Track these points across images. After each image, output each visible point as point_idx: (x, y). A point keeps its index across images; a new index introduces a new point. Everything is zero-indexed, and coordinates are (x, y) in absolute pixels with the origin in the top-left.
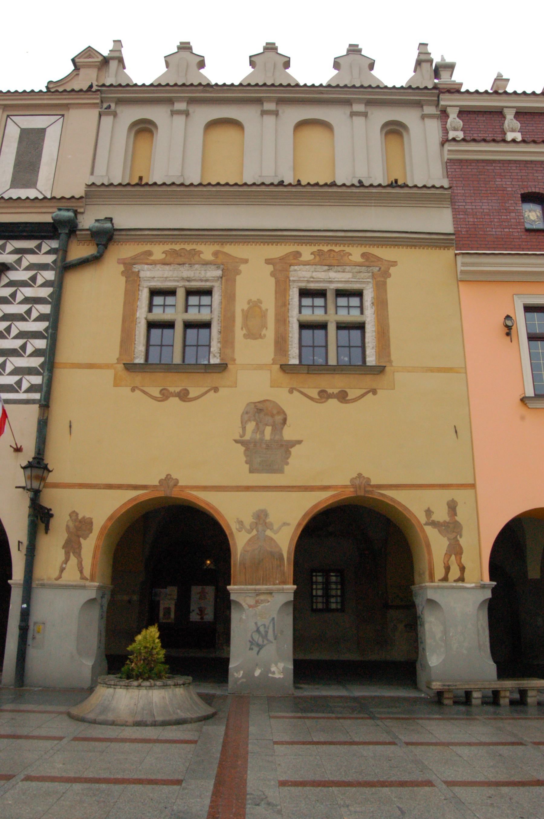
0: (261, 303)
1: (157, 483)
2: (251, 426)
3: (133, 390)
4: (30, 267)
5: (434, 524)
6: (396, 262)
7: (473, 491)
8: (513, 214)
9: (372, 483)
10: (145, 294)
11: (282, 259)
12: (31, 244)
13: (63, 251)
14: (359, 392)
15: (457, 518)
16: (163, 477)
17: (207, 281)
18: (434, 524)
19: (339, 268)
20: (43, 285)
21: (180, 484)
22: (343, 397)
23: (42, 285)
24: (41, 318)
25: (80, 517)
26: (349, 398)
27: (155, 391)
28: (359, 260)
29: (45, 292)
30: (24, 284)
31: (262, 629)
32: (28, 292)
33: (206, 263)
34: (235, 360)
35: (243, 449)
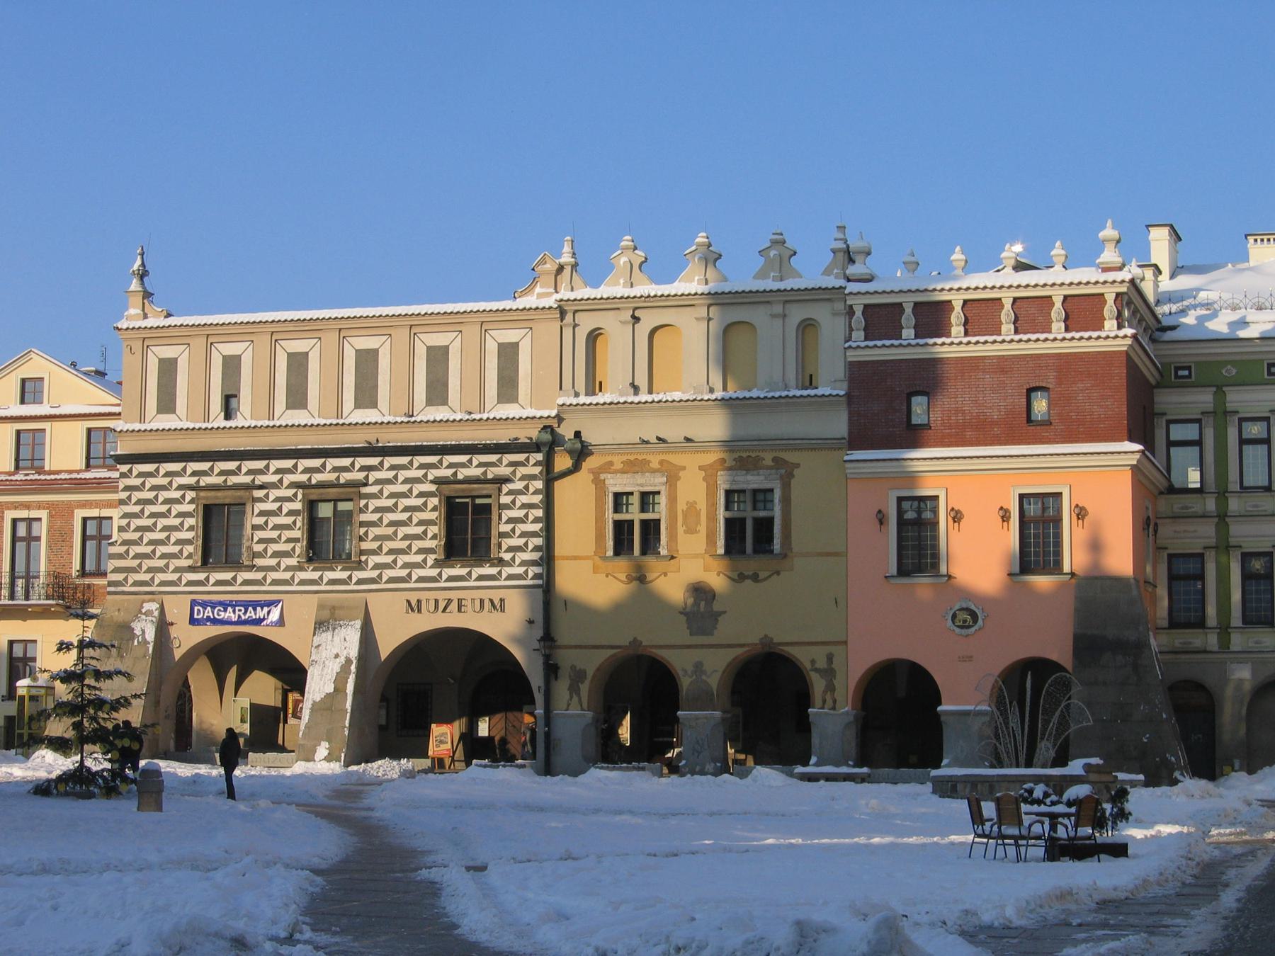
0: (696, 503)
1: (628, 644)
3: (607, 576)
4: (523, 478)
5: (816, 670)
6: (799, 464)
7: (845, 646)
8: (898, 414)
9: (775, 641)
10: (610, 498)
11: (711, 466)
13: (548, 464)
14: (766, 574)
15: (833, 666)
16: (631, 639)
17: (655, 486)
18: (816, 670)
19: (755, 472)
20: (534, 493)
21: (644, 644)
22: (755, 578)
23: (534, 493)
24: (536, 520)
25: (578, 668)
26: (760, 578)
28: (771, 463)
30: (519, 492)
31: (700, 742)
33: (654, 471)
34: (678, 551)
35: (685, 618)
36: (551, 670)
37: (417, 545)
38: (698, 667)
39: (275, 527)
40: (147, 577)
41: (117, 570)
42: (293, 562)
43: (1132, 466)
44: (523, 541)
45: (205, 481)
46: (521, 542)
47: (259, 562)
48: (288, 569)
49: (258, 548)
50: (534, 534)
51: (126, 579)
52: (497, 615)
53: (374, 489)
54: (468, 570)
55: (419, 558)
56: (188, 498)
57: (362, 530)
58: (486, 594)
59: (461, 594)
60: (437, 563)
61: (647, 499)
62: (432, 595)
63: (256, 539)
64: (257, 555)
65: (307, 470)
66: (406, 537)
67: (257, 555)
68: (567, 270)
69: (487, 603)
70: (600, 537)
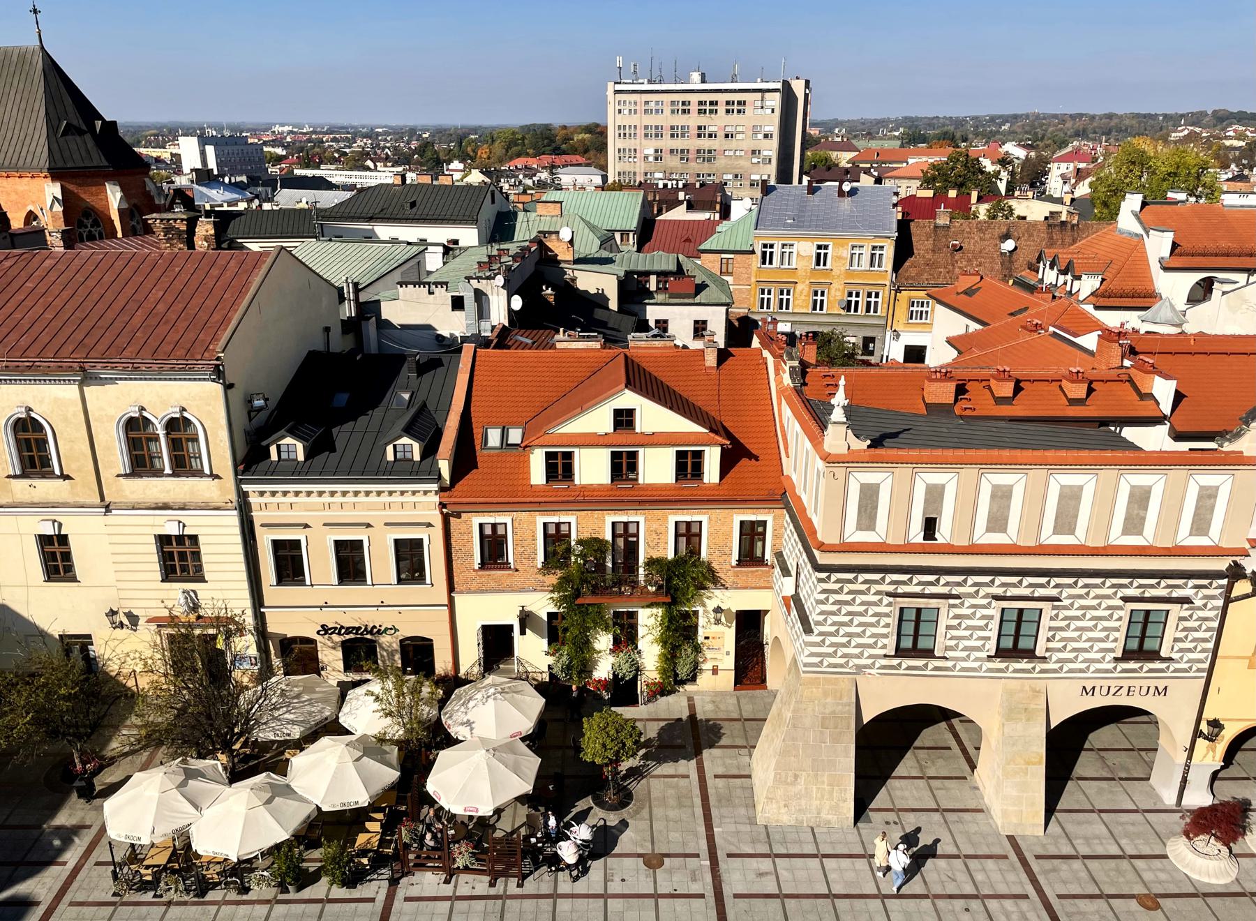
29: (1212, 614)
32: (1201, 614)
37: (1098, 645)
40: (842, 661)
42: (984, 655)
45: (902, 589)
47: (949, 654)
48: (977, 659)
49: (952, 643)
51: (821, 662)
53: (1066, 602)
54: (1140, 665)
58: (1153, 683)
59: (1131, 683)
62: (1106, 683)
63: (948, 636)
64: (947, 648)
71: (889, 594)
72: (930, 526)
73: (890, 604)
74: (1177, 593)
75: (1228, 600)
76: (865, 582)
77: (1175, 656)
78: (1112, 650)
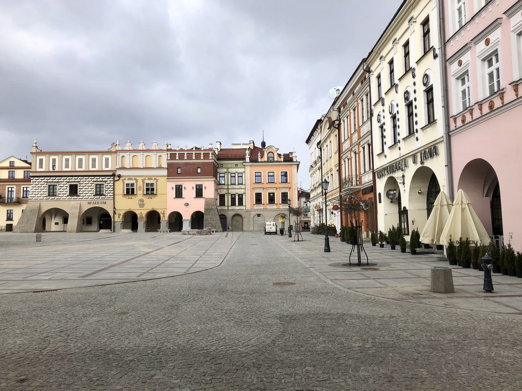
2: (140, 202)
12: (109, 177)
22: (151, 198)
24: (112, 188)
27: (128, 198)
30: (109, 183)
36: (115, 213)
38: (141, 213)
39: (63, 189)
40: (37, 198)
41: (30, 197)
42: (66, 195)
43: (214, 181)
44: (110, 192)
46: (109, 192)
47: (59, 195)
48: (65, 196)
49: (60, 193)
50: (112, 191)
52: (105, 204)
53: (82, 183)
55: (90, 195)
56: (45, 184)
57: (80, 190)
60: (94, 196)
61: (132, 185)
64: (59, 194)
65: (69, 179)
66: (88, 191)
67: (59, 194)
68: (118, 145)
69: (103, 203)
70: (124, 191)
71: (46, 182)
72: (54, 166)
73: (46, 184)
74: (104, 180)
75: (114, 181)
76: (41, 179)
77: (107, 194)
78: (93, 193)
